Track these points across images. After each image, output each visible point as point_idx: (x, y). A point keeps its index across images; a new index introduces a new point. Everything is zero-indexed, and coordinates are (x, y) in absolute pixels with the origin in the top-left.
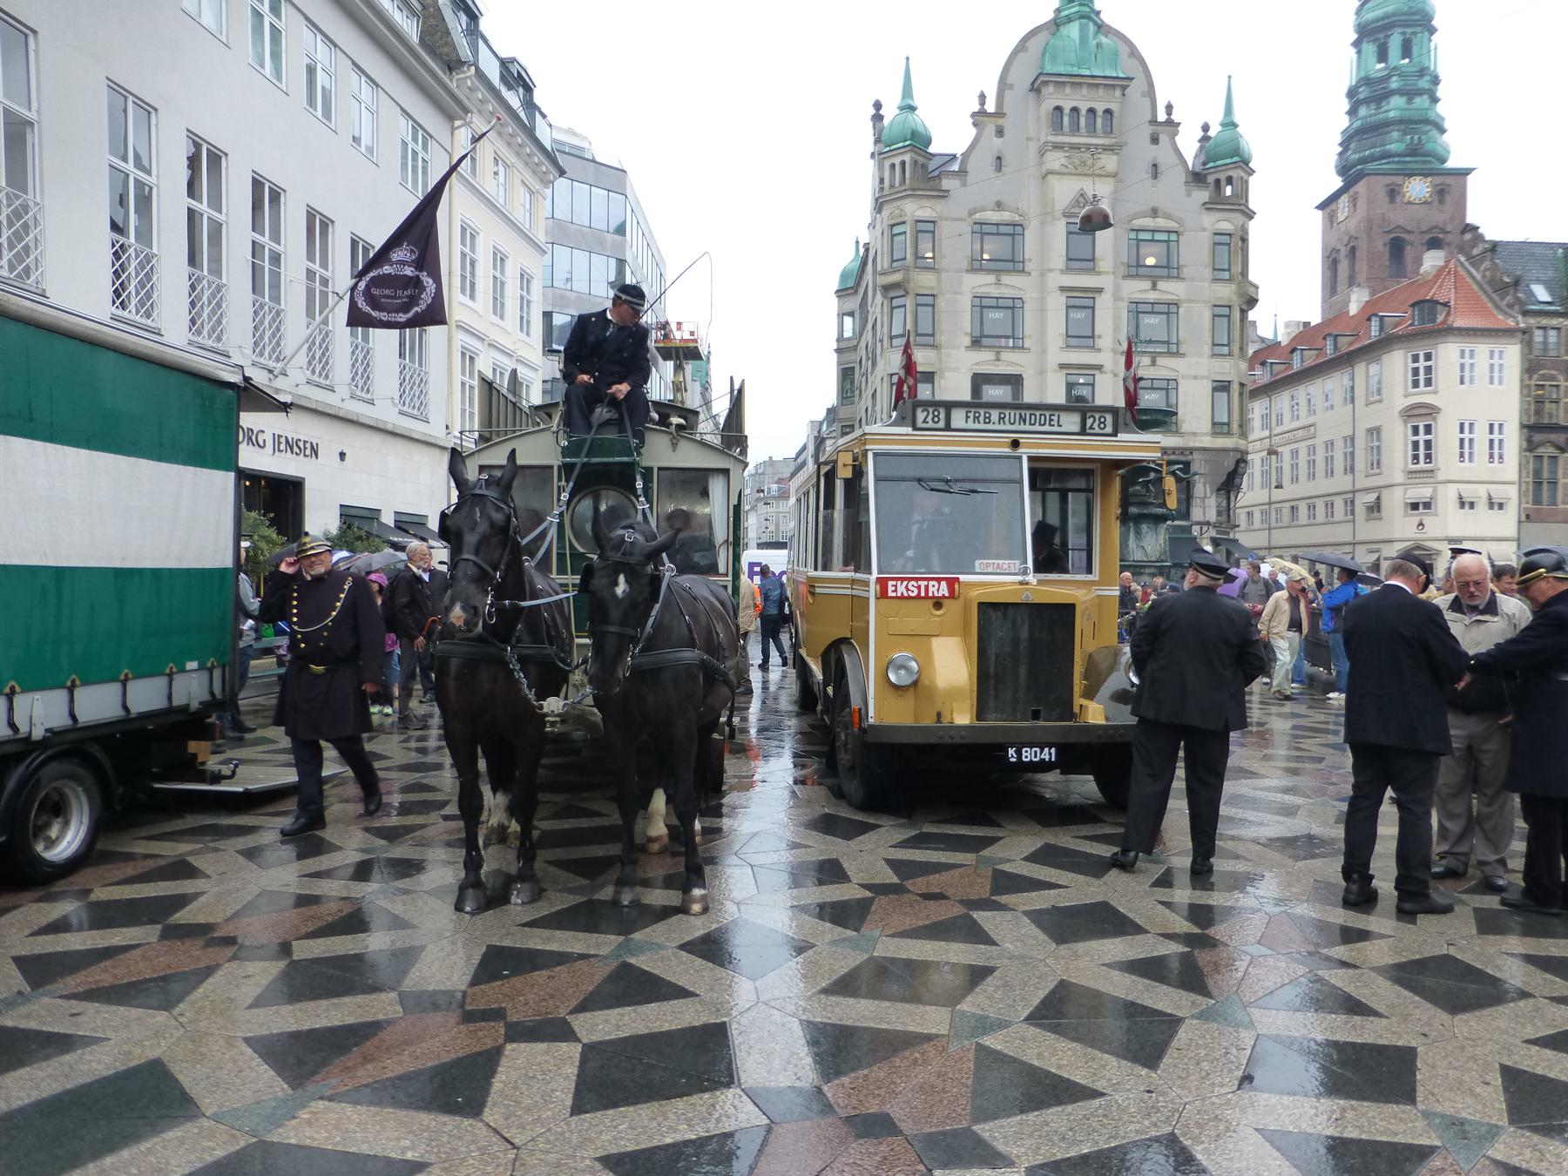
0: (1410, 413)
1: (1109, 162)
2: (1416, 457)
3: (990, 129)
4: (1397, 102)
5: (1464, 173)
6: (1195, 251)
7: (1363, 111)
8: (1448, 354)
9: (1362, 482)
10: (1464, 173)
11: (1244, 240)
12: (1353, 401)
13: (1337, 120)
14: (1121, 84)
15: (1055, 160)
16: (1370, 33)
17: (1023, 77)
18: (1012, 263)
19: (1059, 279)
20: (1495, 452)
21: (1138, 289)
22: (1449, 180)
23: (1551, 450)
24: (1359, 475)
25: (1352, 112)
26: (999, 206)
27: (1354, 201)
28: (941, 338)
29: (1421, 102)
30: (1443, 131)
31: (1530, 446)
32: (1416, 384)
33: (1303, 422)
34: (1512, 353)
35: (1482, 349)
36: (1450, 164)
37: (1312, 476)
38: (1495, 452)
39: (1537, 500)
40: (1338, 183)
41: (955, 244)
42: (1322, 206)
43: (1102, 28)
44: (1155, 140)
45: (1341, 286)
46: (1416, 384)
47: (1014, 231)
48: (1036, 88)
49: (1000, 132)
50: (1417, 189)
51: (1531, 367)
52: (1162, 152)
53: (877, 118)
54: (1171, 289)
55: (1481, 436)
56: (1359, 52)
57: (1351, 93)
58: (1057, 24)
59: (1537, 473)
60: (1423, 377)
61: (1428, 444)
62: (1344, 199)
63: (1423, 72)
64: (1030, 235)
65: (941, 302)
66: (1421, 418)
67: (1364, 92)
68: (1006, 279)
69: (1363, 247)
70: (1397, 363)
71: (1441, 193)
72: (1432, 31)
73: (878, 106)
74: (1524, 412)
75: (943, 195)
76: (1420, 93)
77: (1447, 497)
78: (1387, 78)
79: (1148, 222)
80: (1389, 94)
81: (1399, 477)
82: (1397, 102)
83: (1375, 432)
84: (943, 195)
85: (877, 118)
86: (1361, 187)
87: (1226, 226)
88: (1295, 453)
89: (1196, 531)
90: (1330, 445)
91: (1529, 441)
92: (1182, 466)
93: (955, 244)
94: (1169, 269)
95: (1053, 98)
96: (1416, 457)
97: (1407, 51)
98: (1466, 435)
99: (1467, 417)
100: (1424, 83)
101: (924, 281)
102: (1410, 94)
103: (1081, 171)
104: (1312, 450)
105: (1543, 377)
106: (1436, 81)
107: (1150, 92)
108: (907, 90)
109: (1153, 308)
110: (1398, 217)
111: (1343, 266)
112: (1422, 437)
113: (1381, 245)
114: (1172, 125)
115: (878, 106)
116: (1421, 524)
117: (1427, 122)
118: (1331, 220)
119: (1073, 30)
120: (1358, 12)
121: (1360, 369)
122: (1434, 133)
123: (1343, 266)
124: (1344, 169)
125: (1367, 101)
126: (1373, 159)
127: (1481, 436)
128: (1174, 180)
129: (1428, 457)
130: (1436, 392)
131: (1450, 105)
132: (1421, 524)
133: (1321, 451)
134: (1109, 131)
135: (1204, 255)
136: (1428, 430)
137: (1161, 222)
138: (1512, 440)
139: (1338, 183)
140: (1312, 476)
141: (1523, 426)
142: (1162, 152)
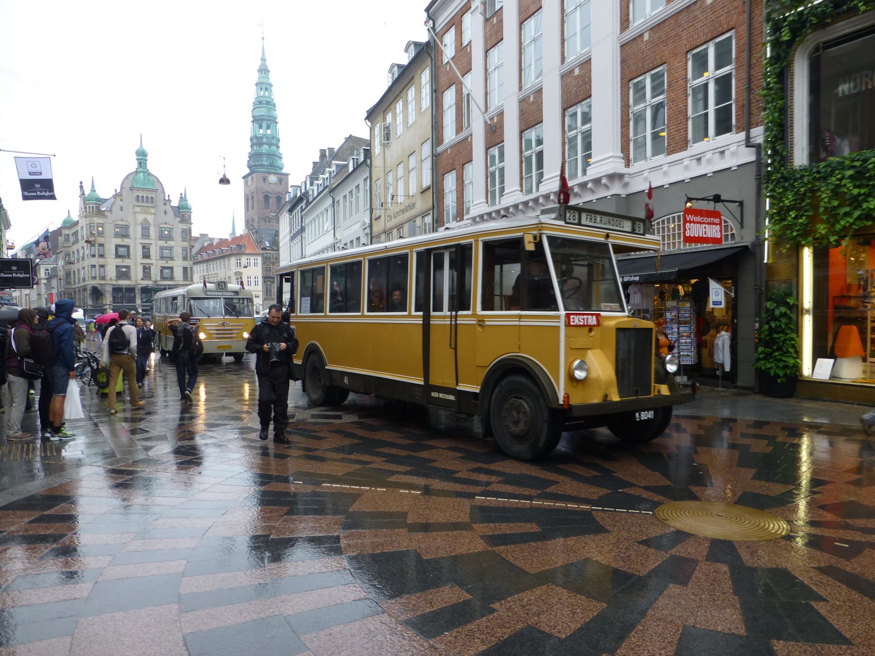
0: (236, 273)
1: (153, 210)
3: (119, 199)
4: (265, 147)
5: (287, 175)
6: (177, 234)
7: (255, 148)
8: (244, 260)
11: (190, 230)
13: (247, 149)
14: (156, 191)
15: (138, 209)
16: (257, 121)
17: (128, 185)
18: (126, 236)
19: (139, 241)
20: (256, 284)
21: (162, 243)
25: (252, 146)
26: (122, 220)
27: (252, 179)
28: (106, 256)
29: (274, 148)
31: (264, 282)
34: (260, 260)
35: (252, 258)
36: (284, 171)
38: (256, 284)
40: (248, 171)
41: (110, 230)
42: (244, 178)
43: (150, 174)
44: (165, 204)
45: (250, 209)
47: (127, 227)
48: (132, 189)
49: (121, 200)
50: (273, 179)
51: (264, 263)
52: (168, 208)
53: (81, 187)
54: (171, 243)
57: (251, 139)
58: (136, 172)
62: (250, 178)
63: (273, 138)
64: (131, 228)
65: (106, 246)
67: (255, 141)
68: (125, 240)
69: (255, 196)
70: (233, 260)
71: (280, 181)
72: (277, 123)
73: (81, 183)
74: (263, 273)
75: (106, 216)
76: (273, 145)
78: (262, 138)
79: (164, 226)
80: (263, 144)
82: (265, 147)
83: (229, 277)
84: (106, 216)
85: (81, 187)
86: (254, 175)
87: (185, 227)
93: (110, 230)
94: (170, 238)
95: (136, 193)
100: (274, 142)
101: (101, 240)
102: (270, 145)
103: (145, 212)
106: (278, 140)
107: (163, 192)
108: (93, 186)
109: (166, 248)
110: (266, 188)
111: (250, 201)
113: (261, 197)
114: (169, 200)
115: (81, 183)
118: (246, 183)
119: (141, 175)
122: (278, 160)
123: (250, 201)
124: (249, 167)
125: (256, 144)
126: (258, 165)
128: (171, 213)
131: (284, 149)
134: (152, 202)
135: (180, 235)
137: (168, 226)
139: (248, 171)
142: (168, 208)
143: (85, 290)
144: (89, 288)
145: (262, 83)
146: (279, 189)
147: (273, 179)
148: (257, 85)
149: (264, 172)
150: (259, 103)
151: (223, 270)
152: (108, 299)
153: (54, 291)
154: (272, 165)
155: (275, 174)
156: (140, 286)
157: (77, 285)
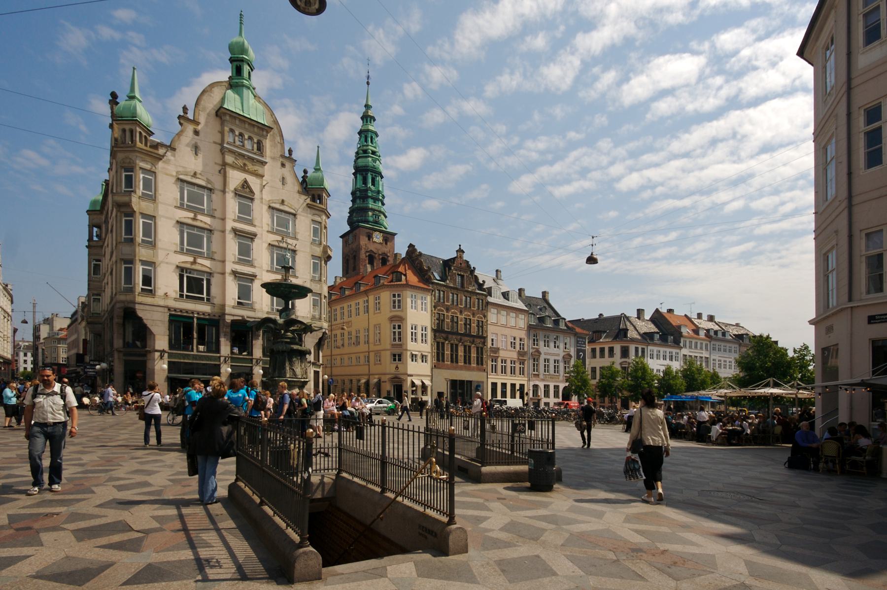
0: (392, 319)
2: (395, 339)
4: (371, 201)
5: (394, 234)
7: (358, 201)
9: (372, 348)
10: (394, 234)
12: (368, 312)
22: (389, 236)
23: (442, 340)
24: (371, 346)
30: (386, 217)
32: (394, 307)
33: (346, 319)
39: (438, 360)
40: (348, 228)
46: (394, 307)
55: (419, 332)
56: (356, 178)
57: (353, 193)
59: (438, 349)
60: (398, 304)
61: (400, 333)
63: (379, 192)
66: (398, 322)
76: (378, 200)
81: (388, 347)
82: (371, 201)
86: (357, 231)
91: (435, 336)
96: (395, 339)
97: (373, 184)
102: (376, 200)
105: (439, 310)
106: (383, 197)
110: (372, 247)
116: (397, 367)
117: (380, 212)
120: (355, 162)
121: (371, 298)
124: (350, 222)
125: (360, 198)
127: (419, 332)
129: (400, 339)
130: (402, 311)
132: (397, 367)
136: (399, 327)
138: (429, 333)
139: (347, 228)
141: (432, 329)
145: (368, 131)
146: (385, 249)
147: (378, 238)
148: (360, 133)
149: (370, 228)
150: (362, 153)
151: (363, 316)
154: (377, 222)
155: (381, 231)
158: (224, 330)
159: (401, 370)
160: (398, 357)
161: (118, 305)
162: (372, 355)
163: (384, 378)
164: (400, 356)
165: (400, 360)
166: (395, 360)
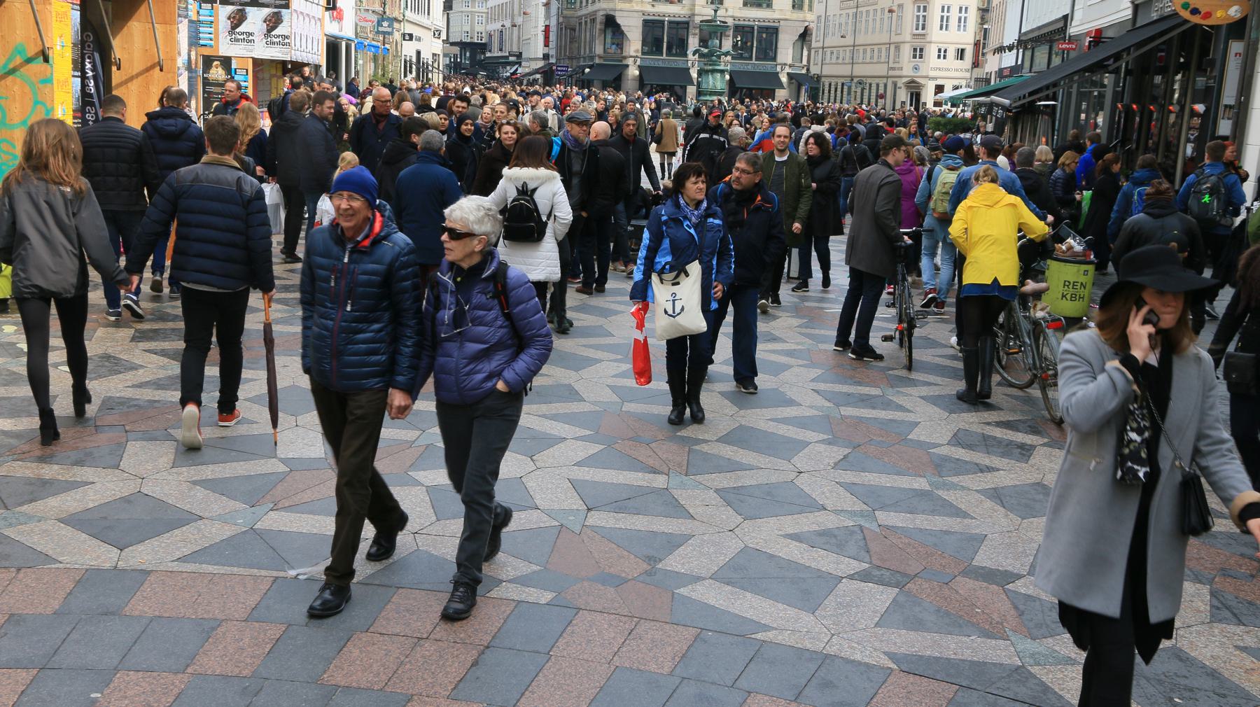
9: (895, 39)
37: (873, 32)
55: (954, 15)
77: (932, 52)
81: (908, 38)
88: (868, 12)
89: (779, 68)
90: (883, 9)
92: (770, 34)
98: (945, 14)
99: (946, 2)
104: (875, 10)
112: (921, 13)
127: (954, 15)
133: (879, 12)
136: (925, 9)
140: (873, 32)
141: (979, 9)
143: (593, 21)
144: (600, 18)
152: (634, 44)
153: (553, 23)
156: (698, 19)
157: (584, 12)
158: (692, 31)
159: (922, 72)
160: (919, 53)
161: (602, 13)
162: (892, 47)
163: (901, 82)
164: (921, 50)
165: (921, 57)
166: (915, 57)
